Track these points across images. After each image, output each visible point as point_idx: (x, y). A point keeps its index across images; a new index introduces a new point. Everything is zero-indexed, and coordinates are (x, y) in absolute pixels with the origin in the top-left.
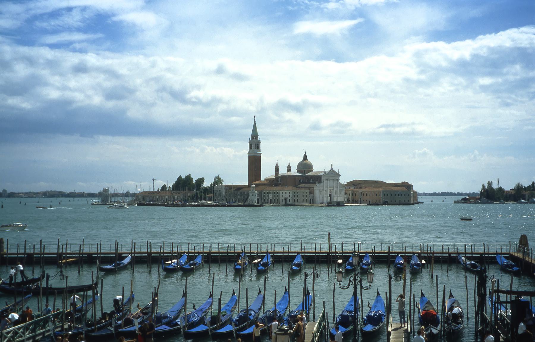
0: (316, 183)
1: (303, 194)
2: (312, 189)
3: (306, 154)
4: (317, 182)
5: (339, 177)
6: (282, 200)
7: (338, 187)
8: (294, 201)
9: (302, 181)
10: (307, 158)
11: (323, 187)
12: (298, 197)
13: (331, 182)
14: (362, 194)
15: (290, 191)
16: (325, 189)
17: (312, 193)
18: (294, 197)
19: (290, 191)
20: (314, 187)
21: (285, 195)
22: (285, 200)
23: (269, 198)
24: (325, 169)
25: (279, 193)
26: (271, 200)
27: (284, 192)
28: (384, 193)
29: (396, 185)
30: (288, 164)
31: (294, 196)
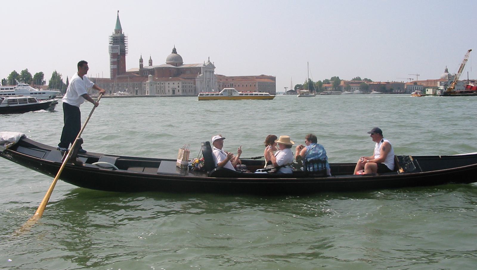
1: (190, 85)
3: (175, 48)
4: (199, 73)
6: (169, 90)
7: (214, 79)
10: (177, 51)
11: (203, 78)
13: (208, 73)
15: (179, 82)
16: (205, 80)
19: (179, 82)
20: (195, 79)
25: (165, 84)
27: (171, 83)
28: (259, 84)
29: (257, 77)
30: (150, 58)
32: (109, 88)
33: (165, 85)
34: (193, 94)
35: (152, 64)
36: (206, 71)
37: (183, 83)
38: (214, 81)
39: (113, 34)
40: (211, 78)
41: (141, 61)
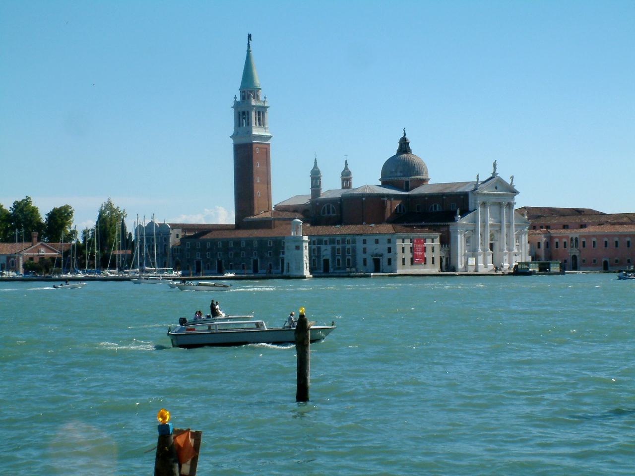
3: (406, 136)
5: (515, 195)
6: (365, 260)
8: (404, 263)
9: (404, 210)
14: (580, 245)
17: (446, 241)
18: (403, 252)
20: (448, 226)
21: (375, 246)
22: (374, 259)
23: (319, 257)
24: (478, 176)
25: (354, 242)
26: (326, 262)
31: (403, 248)
32: (216, 253)
33: (355, 247)
34: (436, 270)
35: (350, 184)
36: (484, 204)
37: (403, 242)
41: (316, 177)
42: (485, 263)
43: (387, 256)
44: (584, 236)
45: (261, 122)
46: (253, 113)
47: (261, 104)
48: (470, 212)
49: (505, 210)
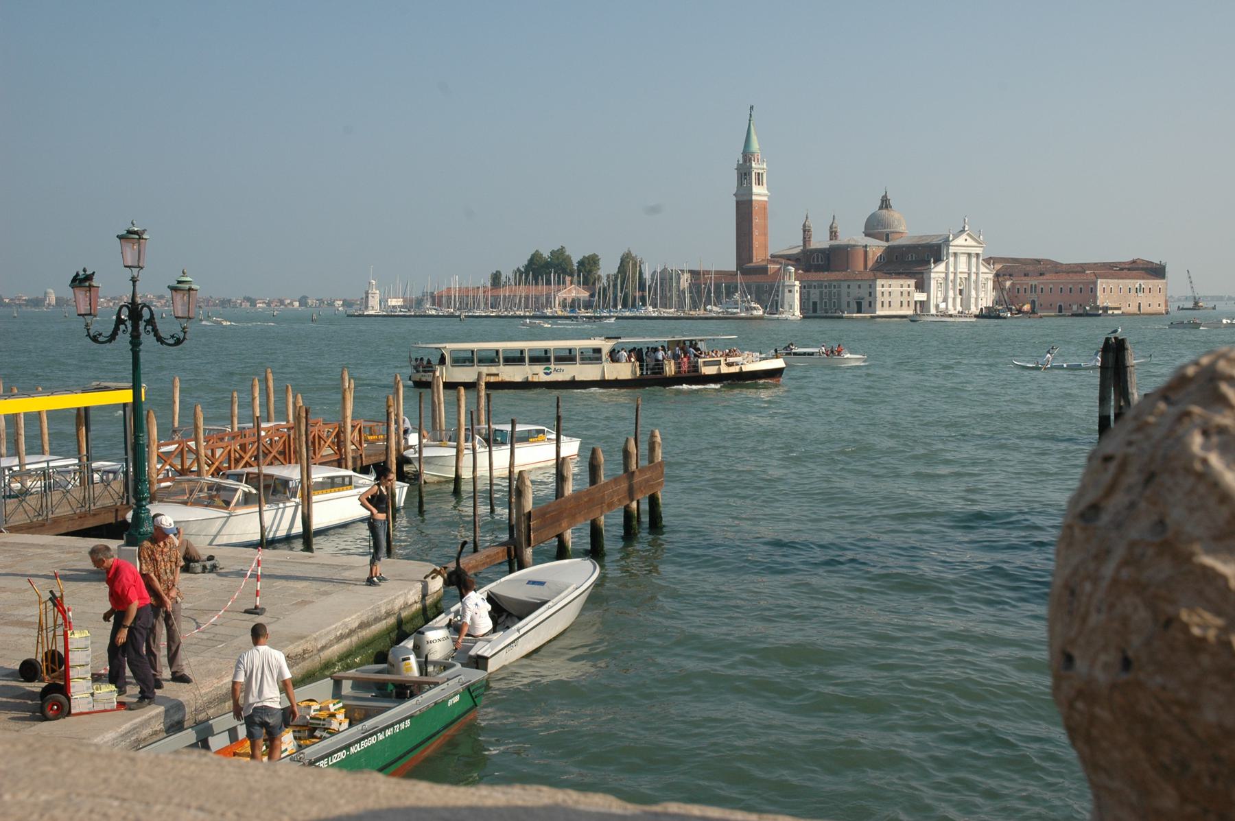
0: (930, 264)
2: (920, 276)
6: (848, 303)
8: (883, 306)
12: (890, 295)
14: (1039, 290)
20: (922, 273)
22: (857, 303)
23: (808, 299)
25: (839, 287)
26: (815, 304)
37: (883, 286)
38: (981, 279)
39: (738, 164)
40: (974, 270)
42: (954, 305)
43: (868, 299)
44: (1042, 283)
45: (759, 183)
46: (753, 174)
47: (761, 166)
48: (943, 260)
49: (974, 260)
